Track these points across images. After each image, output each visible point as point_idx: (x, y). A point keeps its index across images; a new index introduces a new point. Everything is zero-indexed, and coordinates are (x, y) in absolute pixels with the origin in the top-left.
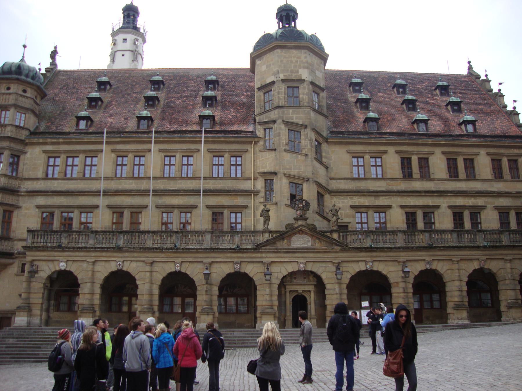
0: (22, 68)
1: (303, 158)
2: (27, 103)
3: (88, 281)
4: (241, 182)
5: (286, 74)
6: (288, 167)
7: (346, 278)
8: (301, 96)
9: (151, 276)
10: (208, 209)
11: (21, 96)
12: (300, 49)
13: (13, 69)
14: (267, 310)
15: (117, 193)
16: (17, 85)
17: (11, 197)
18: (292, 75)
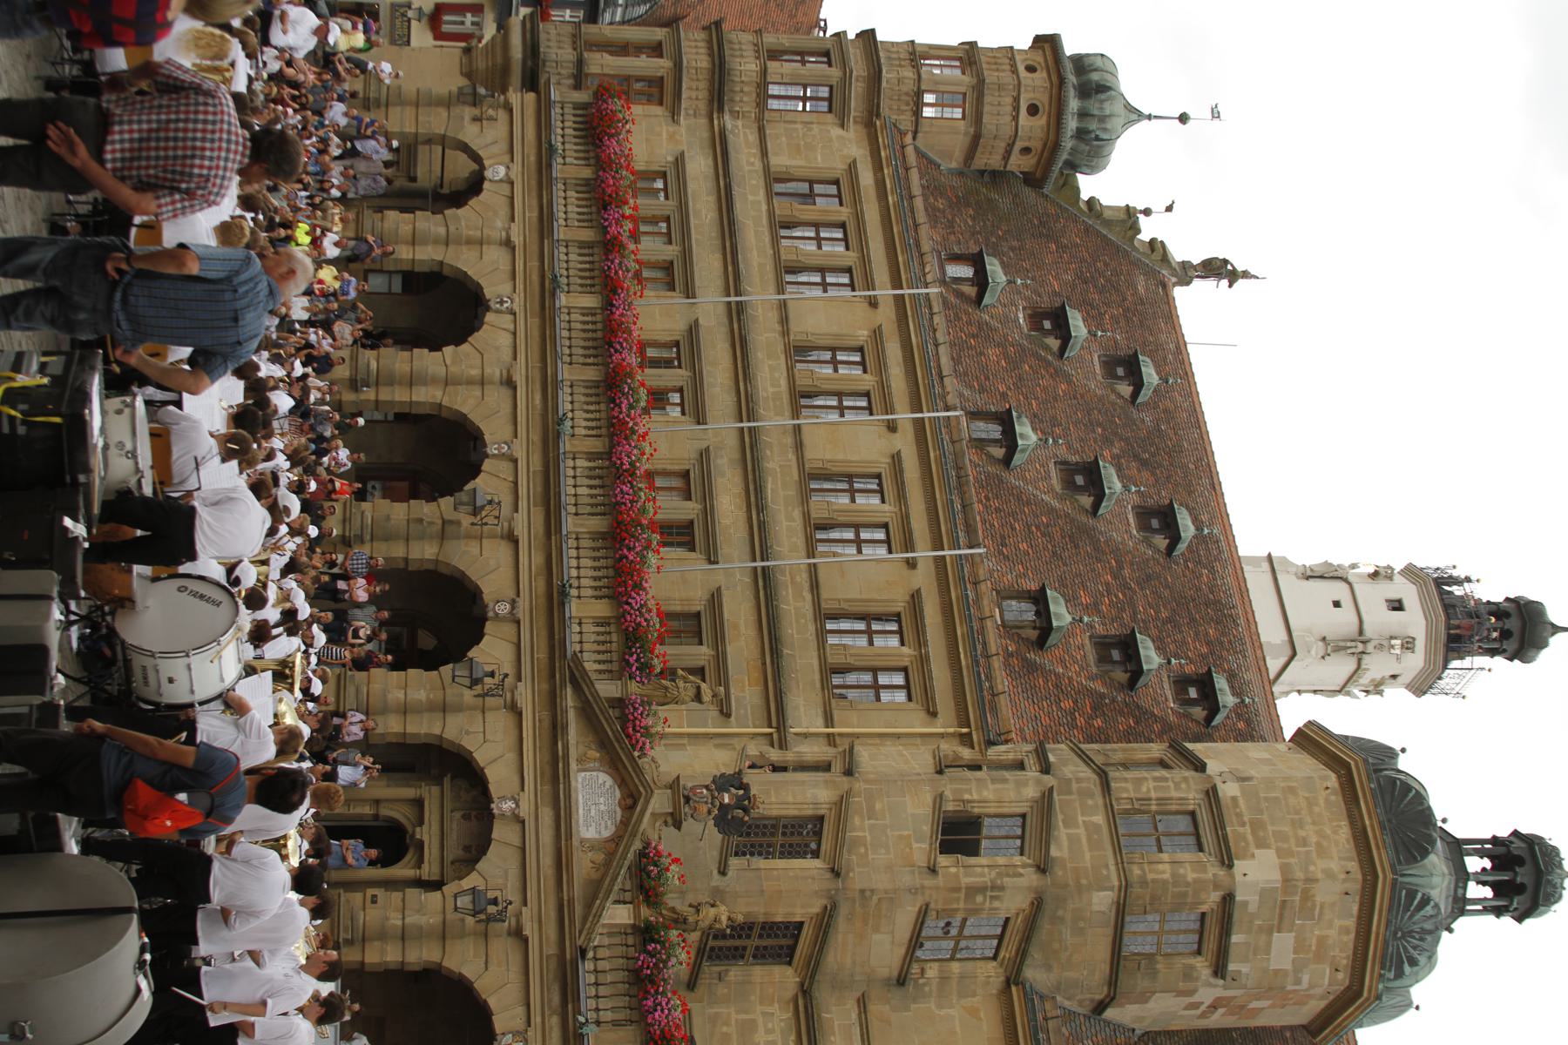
0: (1103, 96)
1: (920, 859)
2: (997, 118)
3: (452, 229)
4: (816, 697)
5: (1241, 802)
6: (878, 806)
7: (464, 960)
8: (1165, 857)
9: (470, 382)
10: (707, 596)
11: (1017, 100)
12: (1359, 854)
13: (1095, 76)
14: (351, 690)
15: (740, 345)
16: (1047, 85)
17: (703, 95)
18: (1243, 824)
